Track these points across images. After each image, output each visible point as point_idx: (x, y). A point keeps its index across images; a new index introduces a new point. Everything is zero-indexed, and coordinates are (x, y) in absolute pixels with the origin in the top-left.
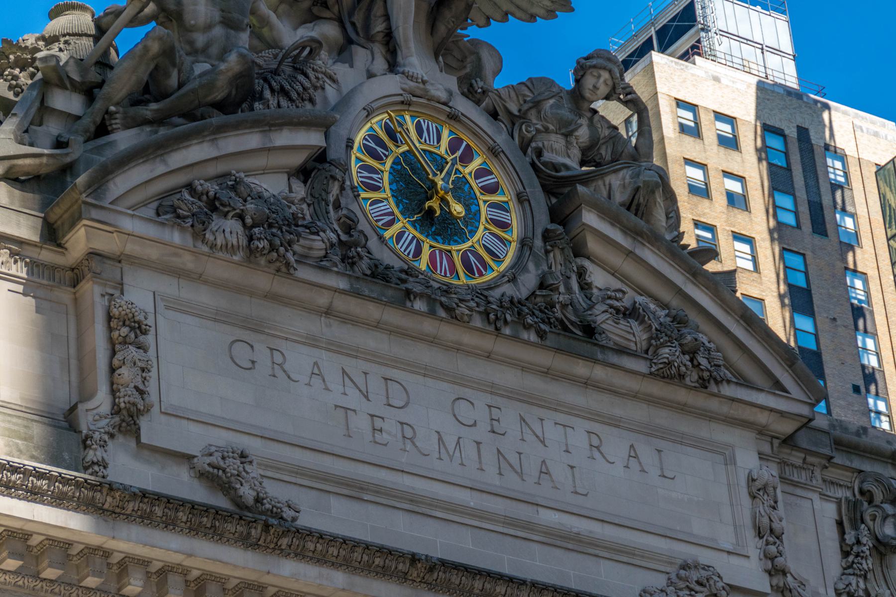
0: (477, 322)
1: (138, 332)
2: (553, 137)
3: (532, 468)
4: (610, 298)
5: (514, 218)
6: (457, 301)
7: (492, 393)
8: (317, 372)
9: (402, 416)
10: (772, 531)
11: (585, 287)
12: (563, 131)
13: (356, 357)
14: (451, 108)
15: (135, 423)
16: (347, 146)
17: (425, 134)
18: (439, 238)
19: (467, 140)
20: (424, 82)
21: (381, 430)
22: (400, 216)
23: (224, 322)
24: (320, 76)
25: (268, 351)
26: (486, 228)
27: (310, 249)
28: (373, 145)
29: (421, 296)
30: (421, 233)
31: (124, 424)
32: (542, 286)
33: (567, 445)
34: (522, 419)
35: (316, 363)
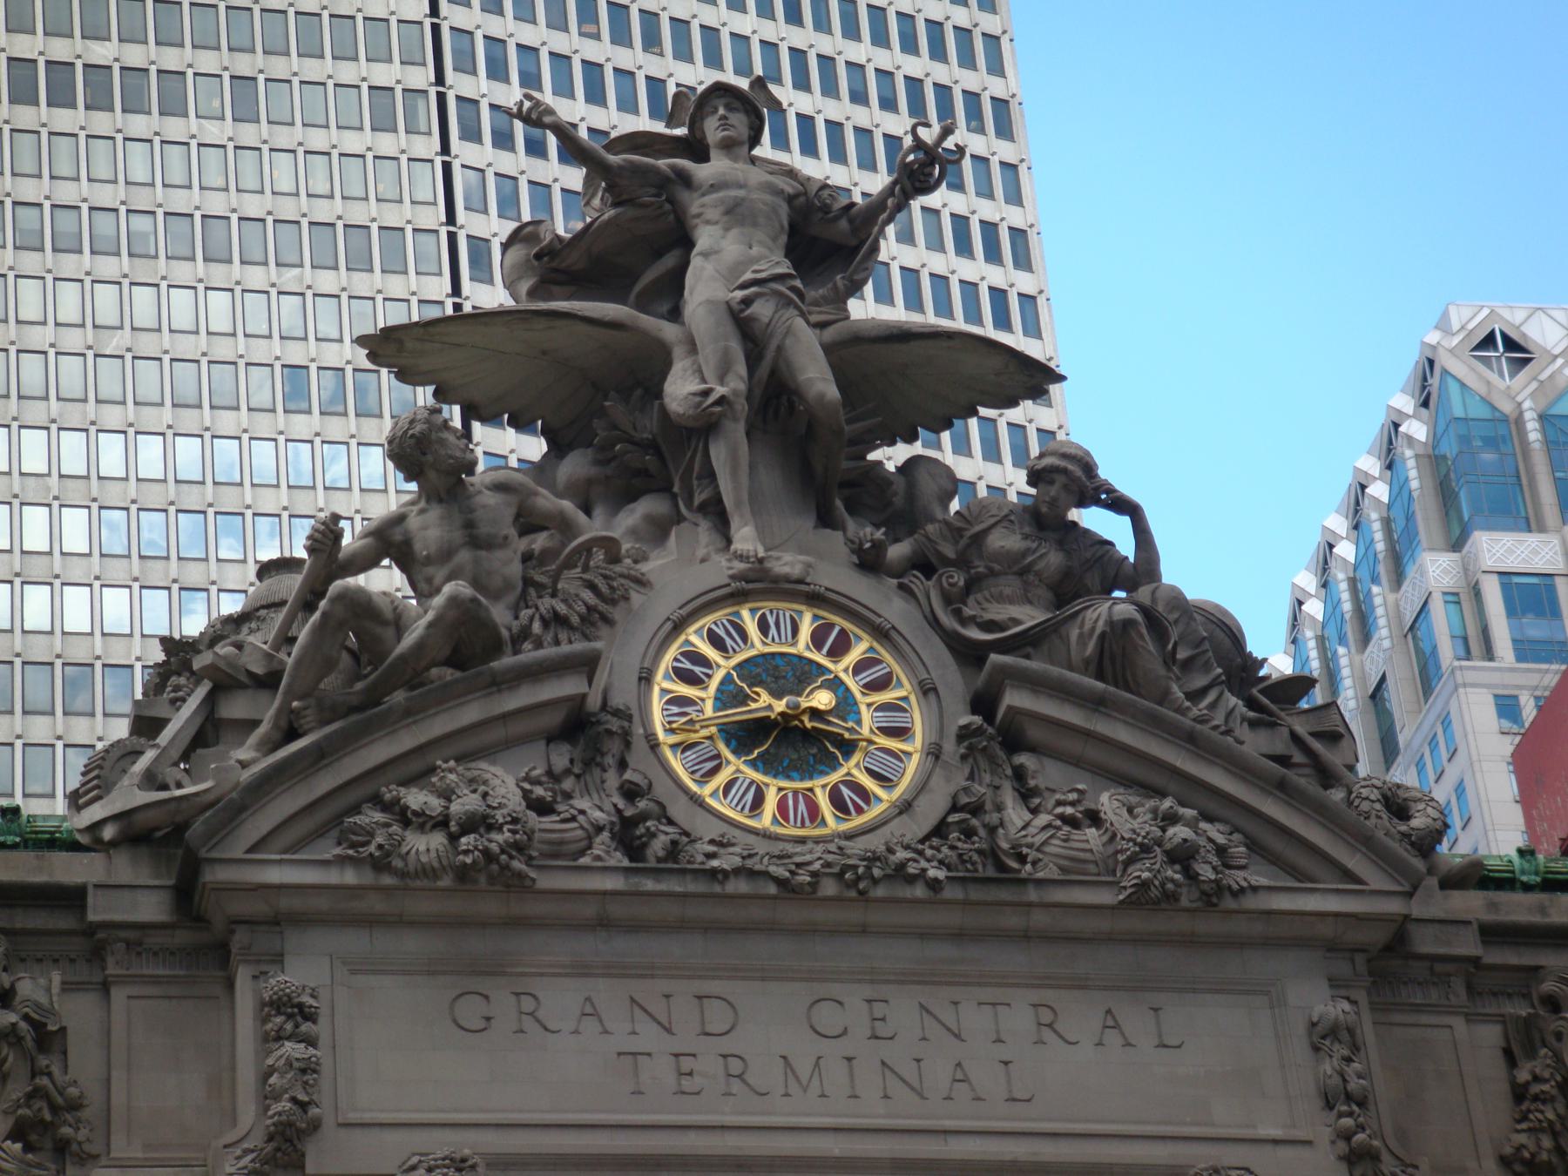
0: (829, 888)
1: (299, 1019)
3: (939, 1074)
4: (1059, 803)
7: (872, 982)
9: (726, 1045)
10: (1349, 1097)
12: (1015, 569)
13: (653, 976)
15: (296, 1150)
16: (640, 679)
17: (773, 630)
18: (794, 774)
19: (840, 622)
20: (761, 561)
21: (690, 1074)
22: (731, 757)
23: (444, 973)
25: (513, 998)
27: (561, 843)
28: (688, 665)
30: (766, 773)
31: (279, 1155)
32: (955, 808)
33: (998, 1032)
35: (588, 999)
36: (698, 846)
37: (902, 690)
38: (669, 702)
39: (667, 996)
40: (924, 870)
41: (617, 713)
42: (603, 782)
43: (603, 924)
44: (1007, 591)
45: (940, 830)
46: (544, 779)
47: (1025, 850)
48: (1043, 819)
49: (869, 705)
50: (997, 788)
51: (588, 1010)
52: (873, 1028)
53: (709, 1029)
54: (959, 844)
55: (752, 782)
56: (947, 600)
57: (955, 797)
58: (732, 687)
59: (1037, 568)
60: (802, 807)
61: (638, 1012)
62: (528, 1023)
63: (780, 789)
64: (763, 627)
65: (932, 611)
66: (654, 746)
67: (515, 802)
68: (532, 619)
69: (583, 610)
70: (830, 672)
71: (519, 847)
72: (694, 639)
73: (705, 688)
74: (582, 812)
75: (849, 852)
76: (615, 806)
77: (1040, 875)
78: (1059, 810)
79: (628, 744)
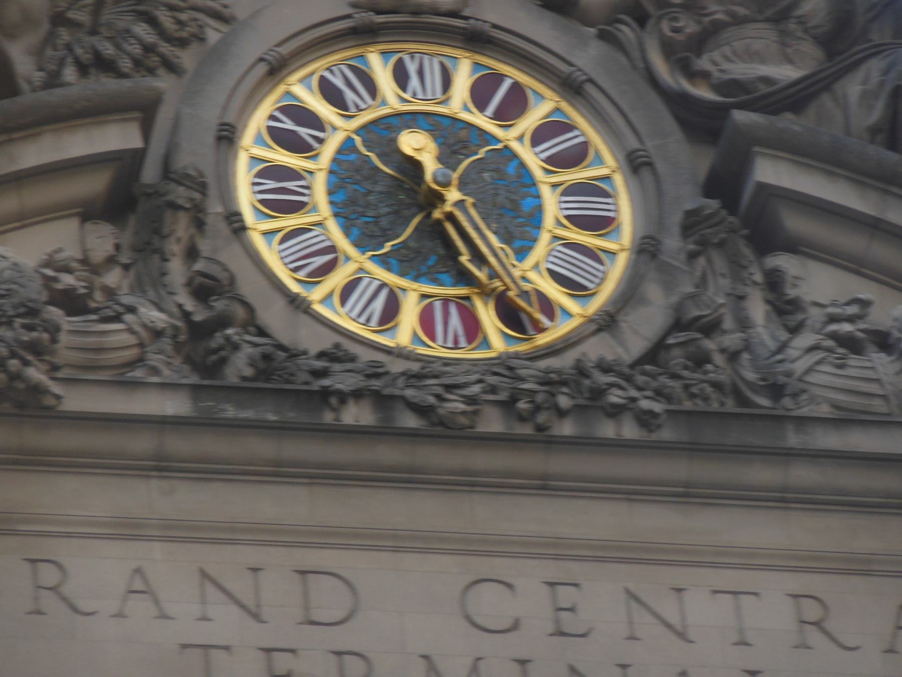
0: (493, 422)
2: (751, 29)
4: (833, 319)
5: (625, 209)
6: (439, 390)
7: (556, 557)
8: (141, 587)
11: (786, 309)
12: (769, 13)
14: (466, 18)
16: (220, 139)
17: (414, 82)
19: (513, 74)
22: (351, 251)
24: (183, 16)
25: (27, 566)
26: (556, 238)
28: (289, 125)
29: (358, 394)
30: (402, 275)
32: (678, 325)
33: (741, 631)
34: (632, 596)
36: (301, 361)
37: (606, 163)
38: (259, 175)
39: (255, 570)
40: (633, 400)
41: (184, 180)
42: (164, 274)
43: (162, 466)
44: (757, 45)
45: (655, 354)
46: (75, 265)
47: (782, 379)
48: (805, 339)
49: (555, 186)
50: (741, 298)
51: (138, 585)
52: (557, 622)
53: (318, 616)
54: (686, 373)
55: (383, 285)
56: (668, 49)
57: (678, 308)
58: (353, 157)
59: (799, 12)
60: (455, 321)
61: (210, 589)
62: (48, 601)
63: (424, 296)
64: (401, 77)
65: (645, 60)
66: (238, 228)
67: (35, 291)
68: (61, 63)
69: (137, 50)
70: (499, 141)
71: (36, 349)
72: (299, 90)
73: (314, 157)
74: (132, 310)
75: (523, 372)
76: (180, 306)
77: (805, 411)
78: (833, 327)
79: (199, 224)
